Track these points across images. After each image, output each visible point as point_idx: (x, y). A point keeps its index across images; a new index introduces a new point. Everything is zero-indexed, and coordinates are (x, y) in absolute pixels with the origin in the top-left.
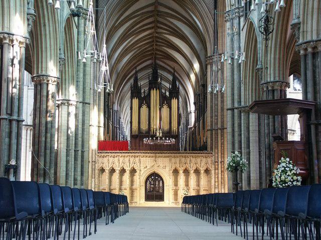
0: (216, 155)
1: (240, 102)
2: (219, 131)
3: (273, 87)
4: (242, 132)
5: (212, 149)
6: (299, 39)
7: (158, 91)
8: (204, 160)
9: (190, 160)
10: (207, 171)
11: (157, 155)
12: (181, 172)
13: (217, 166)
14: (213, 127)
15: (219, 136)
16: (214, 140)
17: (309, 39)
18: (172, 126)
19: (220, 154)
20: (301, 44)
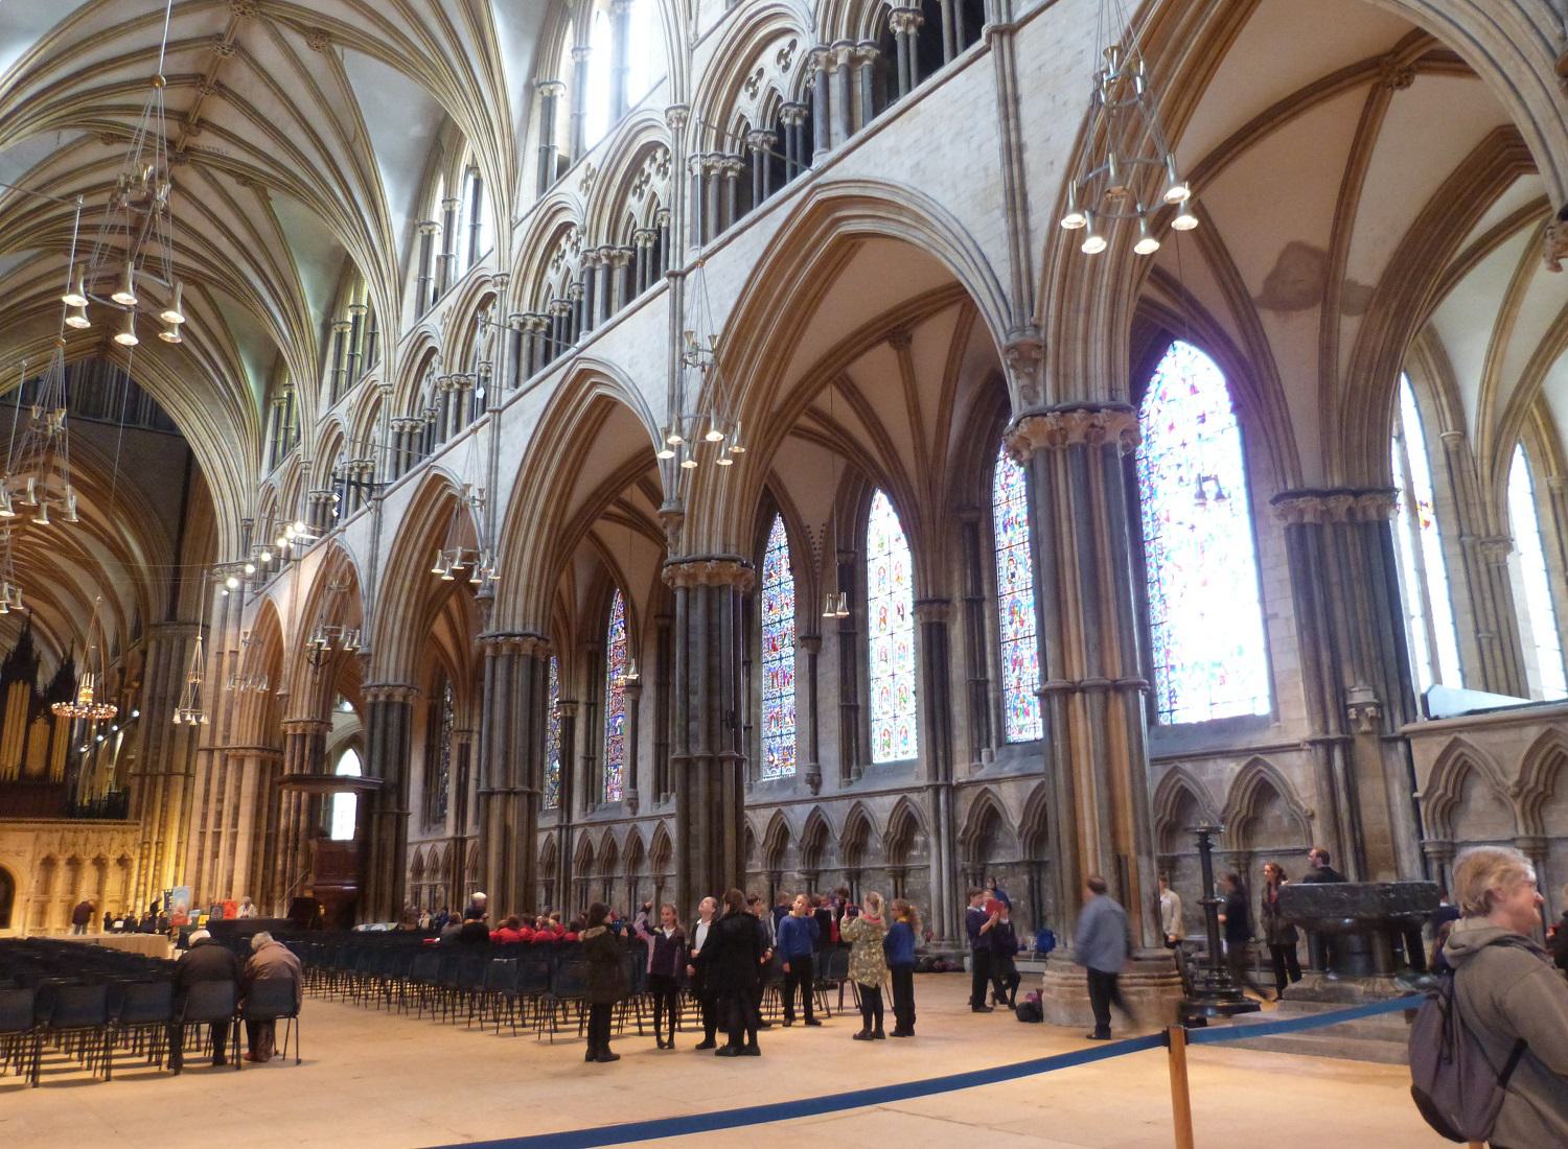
0: (148, 829)
1: (226, 738)
2: (161, 779)
3: (304, 730)
4: (226, 796)
5: (138, 815)
6: (367, 676)
7: (28, 687)
8: (118, 838)
9: (87, 839)
10: (123, 862)
11: (8, 825)
12: (62, 863)
13: (146, 852)
14: (148, 769)
15: (160, 789)
16: (146, 795)
17: (382, 681)
18: (54, 761)
19: (156, 825)
20: (370, 687)
